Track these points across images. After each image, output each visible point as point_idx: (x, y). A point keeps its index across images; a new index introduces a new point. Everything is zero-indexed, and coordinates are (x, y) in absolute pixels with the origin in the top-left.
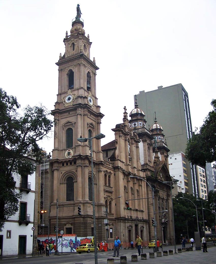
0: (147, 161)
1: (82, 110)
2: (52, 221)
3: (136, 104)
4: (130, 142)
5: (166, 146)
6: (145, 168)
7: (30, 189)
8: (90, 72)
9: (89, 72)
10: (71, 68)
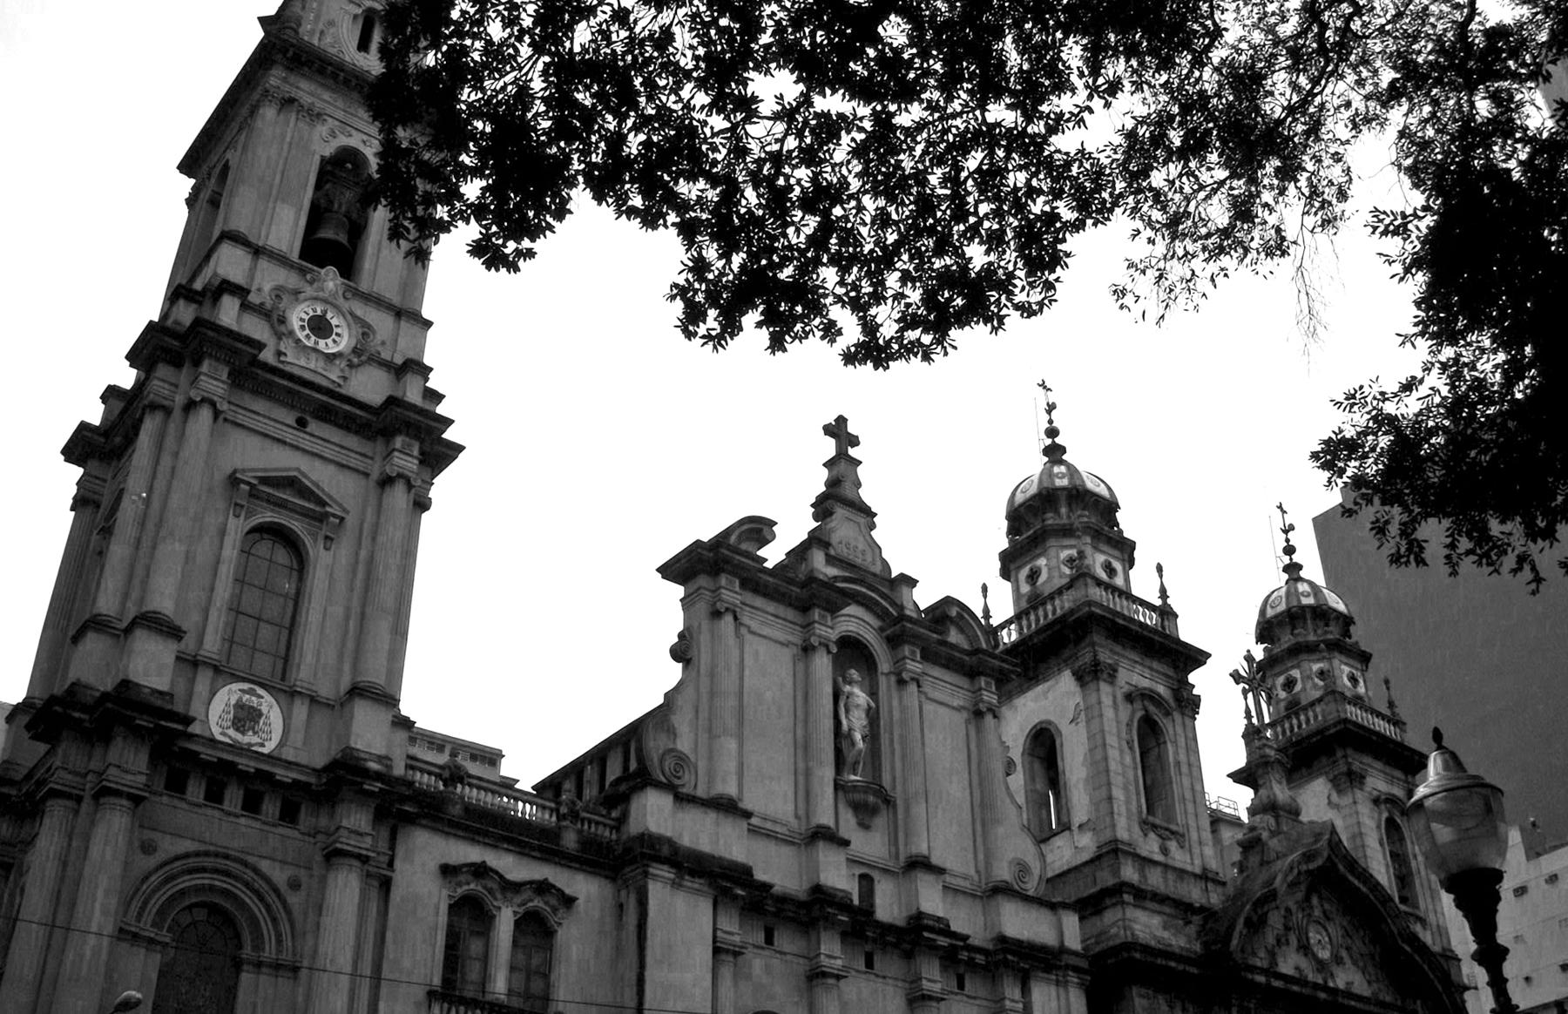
3: (1049, 442)
4: (884, 665)
6: (1106, 879)
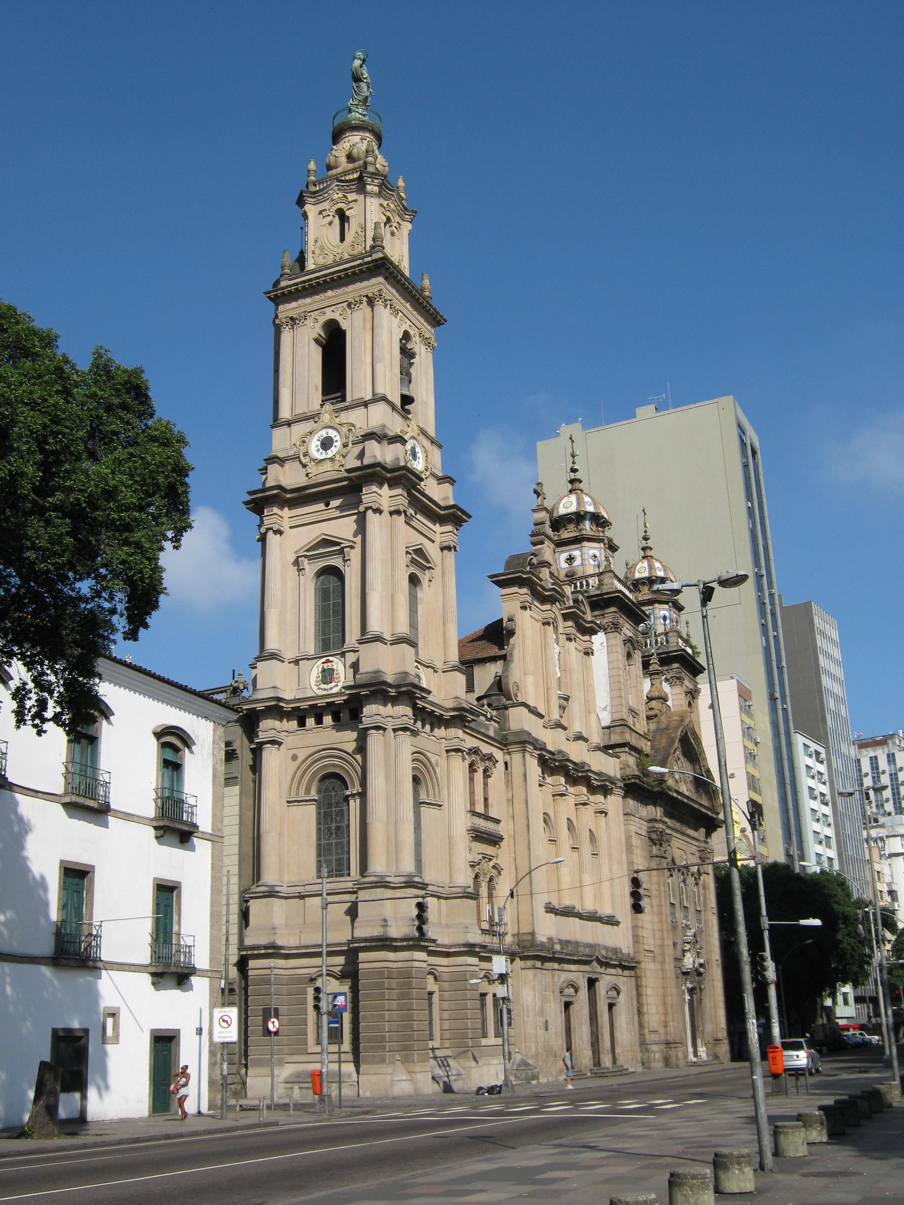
0: (625, 710)
1: (385, 491)
2: (252, 963)
3: (572, 476)
4: (561, 630)
5: (689, 651)
6: (616, 739)
7: (196, 826)
8: (412, 332)
9: (406, 336)
10: (329, 315)
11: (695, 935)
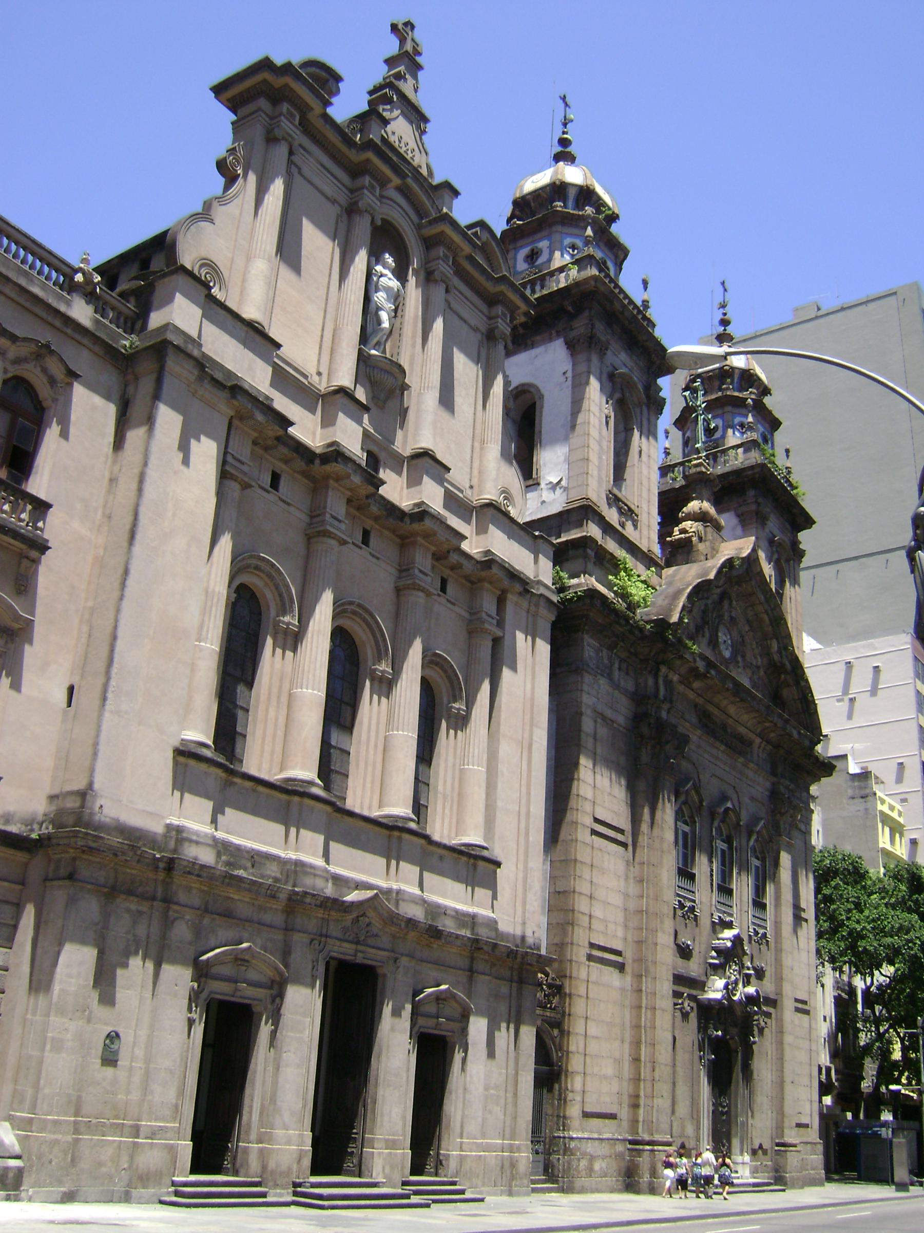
3: (560, 149)
11: (737, 940)
